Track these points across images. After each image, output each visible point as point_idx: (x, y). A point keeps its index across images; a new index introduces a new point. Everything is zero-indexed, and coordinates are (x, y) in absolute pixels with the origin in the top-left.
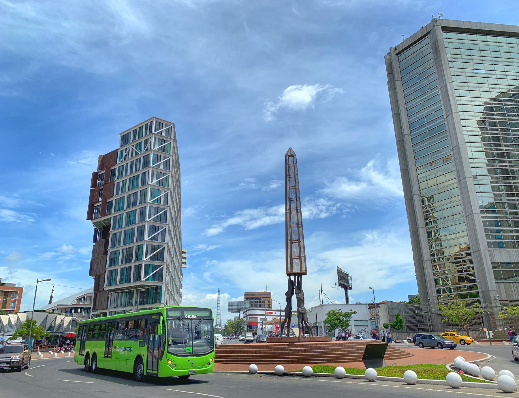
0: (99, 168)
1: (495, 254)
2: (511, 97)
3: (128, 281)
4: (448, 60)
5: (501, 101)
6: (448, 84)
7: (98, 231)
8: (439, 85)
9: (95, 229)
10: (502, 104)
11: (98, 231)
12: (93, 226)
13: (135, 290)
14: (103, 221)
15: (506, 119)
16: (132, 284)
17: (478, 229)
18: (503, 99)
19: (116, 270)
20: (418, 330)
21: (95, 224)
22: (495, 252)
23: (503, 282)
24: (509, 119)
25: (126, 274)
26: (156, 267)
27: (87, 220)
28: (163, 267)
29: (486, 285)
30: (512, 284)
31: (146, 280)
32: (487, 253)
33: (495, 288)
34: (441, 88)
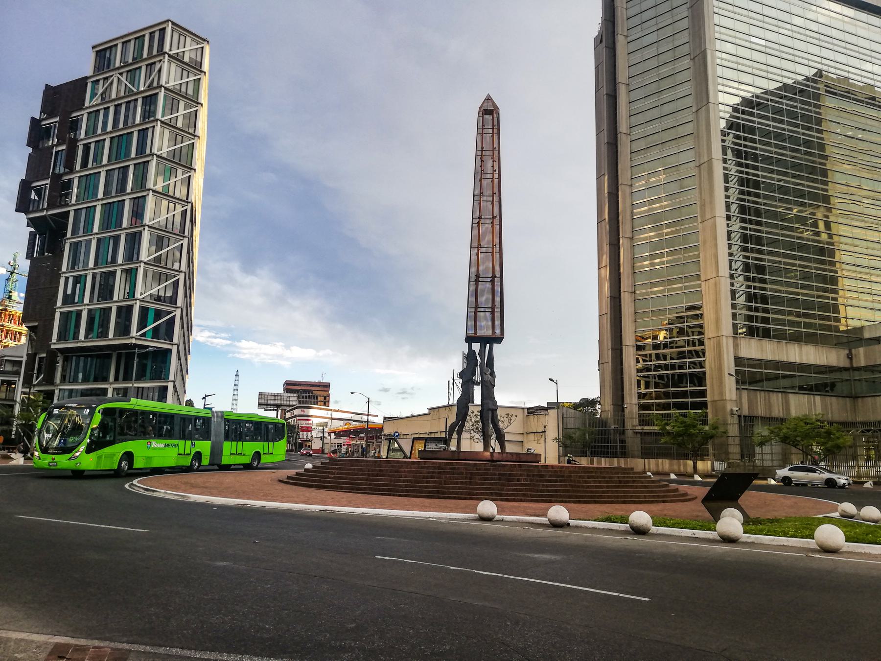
0: (43, 111)
1: (742, 343)
2: (795, 94)
3: (104, 334)
4: (714, 11)
5: (781, 98)
6: (709, 52)
7: (38, 236)
8: (692, 53)
10: (782, 103)
11: (38, 236)
12: (28, 225)
13: (114, 353)
14: (49, 217)
15: (784, 129)
16: (112, 338)
17: (723, 301)
18: (785, 96)
19: (79, 314)
21: (32, 222)
23: (746, 389)
24: (789, 131)
25: (98, 322)
26: (158, 314)
27: (17, 211)
28: (175, 315)
29: (722, 393)
30: (758, 392)
31: (140, 335)
32: (731, 341)
33: (734, 397)
34: (694, 58)
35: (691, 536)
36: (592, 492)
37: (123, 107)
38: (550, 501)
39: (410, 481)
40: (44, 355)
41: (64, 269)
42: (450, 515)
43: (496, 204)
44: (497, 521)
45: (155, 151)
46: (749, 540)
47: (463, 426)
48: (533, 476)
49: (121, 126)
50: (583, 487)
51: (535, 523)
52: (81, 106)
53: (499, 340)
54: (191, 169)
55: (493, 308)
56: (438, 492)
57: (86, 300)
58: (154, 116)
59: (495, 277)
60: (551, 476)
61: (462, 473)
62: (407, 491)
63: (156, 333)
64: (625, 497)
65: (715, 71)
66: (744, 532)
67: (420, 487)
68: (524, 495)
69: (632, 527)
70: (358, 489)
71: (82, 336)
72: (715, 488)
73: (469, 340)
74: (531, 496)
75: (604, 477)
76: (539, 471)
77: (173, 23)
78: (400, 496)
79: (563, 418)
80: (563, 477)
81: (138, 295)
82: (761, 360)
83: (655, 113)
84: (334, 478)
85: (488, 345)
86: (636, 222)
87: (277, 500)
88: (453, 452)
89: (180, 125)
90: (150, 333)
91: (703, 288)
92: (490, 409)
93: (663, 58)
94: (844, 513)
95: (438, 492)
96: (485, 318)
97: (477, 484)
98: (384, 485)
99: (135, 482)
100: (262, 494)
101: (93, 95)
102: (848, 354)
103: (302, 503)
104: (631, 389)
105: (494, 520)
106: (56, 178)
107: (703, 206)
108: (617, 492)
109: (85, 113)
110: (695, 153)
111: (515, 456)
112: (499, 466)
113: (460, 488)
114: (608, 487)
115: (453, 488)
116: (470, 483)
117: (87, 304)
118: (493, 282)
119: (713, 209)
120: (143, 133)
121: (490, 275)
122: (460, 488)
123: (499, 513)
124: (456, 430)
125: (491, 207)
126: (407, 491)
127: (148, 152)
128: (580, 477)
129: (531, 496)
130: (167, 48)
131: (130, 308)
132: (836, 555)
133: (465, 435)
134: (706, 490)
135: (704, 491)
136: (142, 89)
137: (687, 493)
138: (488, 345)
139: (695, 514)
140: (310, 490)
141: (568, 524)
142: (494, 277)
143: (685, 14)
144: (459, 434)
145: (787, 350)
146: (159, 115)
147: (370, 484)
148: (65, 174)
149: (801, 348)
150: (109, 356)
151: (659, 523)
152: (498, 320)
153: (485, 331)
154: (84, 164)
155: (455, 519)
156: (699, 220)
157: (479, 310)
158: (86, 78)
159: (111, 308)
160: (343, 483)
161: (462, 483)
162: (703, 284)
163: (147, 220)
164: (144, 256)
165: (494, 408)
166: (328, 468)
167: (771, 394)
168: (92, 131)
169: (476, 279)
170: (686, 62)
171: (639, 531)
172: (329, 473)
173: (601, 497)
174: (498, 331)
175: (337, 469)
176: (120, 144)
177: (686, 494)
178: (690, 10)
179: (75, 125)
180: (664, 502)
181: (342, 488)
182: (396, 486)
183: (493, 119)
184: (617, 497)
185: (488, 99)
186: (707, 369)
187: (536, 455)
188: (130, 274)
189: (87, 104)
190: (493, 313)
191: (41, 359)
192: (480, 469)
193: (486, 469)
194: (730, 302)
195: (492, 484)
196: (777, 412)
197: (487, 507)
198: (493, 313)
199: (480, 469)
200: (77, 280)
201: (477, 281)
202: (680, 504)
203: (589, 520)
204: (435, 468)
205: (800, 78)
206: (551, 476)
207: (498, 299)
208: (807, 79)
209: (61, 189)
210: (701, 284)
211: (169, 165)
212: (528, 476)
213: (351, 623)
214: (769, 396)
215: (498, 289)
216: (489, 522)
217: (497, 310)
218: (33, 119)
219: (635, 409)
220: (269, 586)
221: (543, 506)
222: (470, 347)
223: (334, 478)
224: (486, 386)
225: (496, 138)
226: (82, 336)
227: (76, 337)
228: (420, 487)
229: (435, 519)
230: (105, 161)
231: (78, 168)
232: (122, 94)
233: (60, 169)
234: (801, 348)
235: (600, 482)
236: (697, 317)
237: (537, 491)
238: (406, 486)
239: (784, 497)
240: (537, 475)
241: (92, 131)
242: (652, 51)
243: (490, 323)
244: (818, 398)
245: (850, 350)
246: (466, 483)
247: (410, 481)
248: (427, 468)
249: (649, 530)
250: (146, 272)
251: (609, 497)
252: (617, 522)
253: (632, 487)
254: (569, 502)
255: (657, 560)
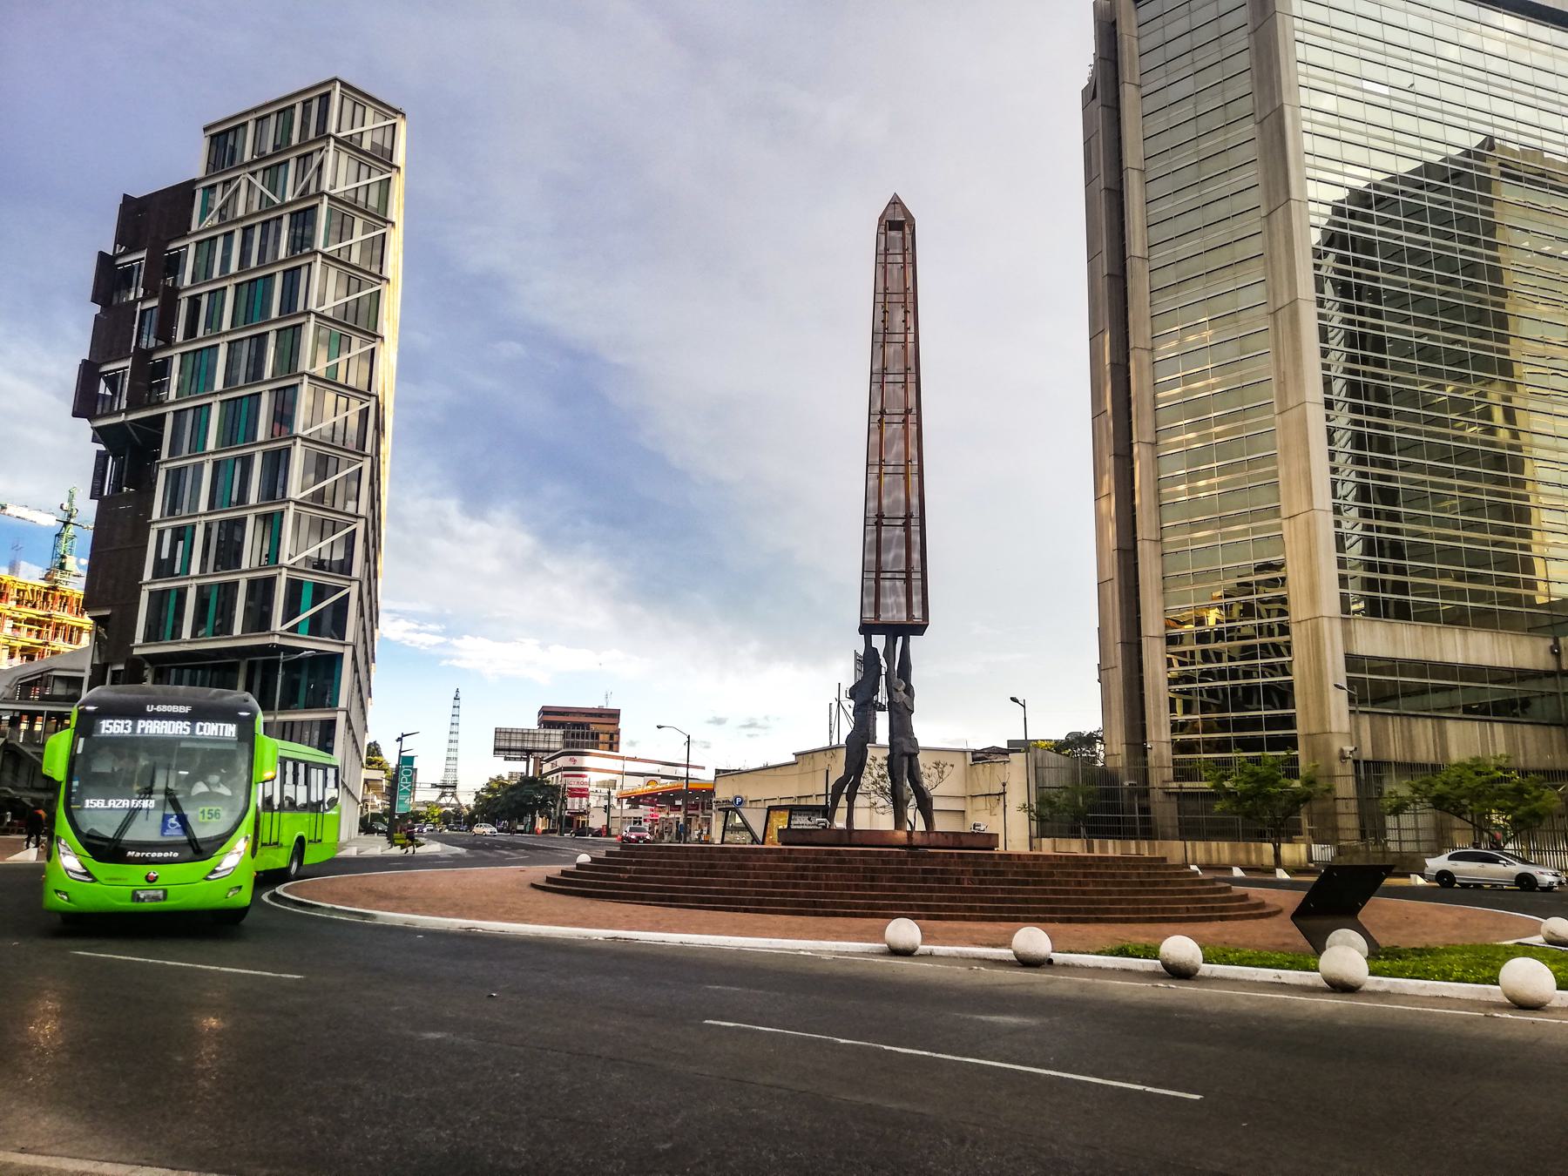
0: (119, 240)
1: (1357, 627)
2: (1446, 181)
3: (225, 628)
5: (1421, 188)
6: (1288, 110)
9: (99, 453)
10: (1421, 197)
12: (94, 440)
15: (1427, 244)
16: (239, 637)
18: (1428, 185)
19: (181, 593)
20: (1120, 833)
21: (100, 435)
22: (1357, 624)
24: (1436, 246)
25: (214, 608)
26: (320, 592)
27: (75, 415)
28: (348, 594)
29: (1323, 719)
30: (1390, 718)
31: (288, 630)
32: (1337, 625)
34: (1261, 121)
35: (1274, 980)
36: (1092, 902)
37: (258, 231)
38: (1016, 920)
39: (764, 885)
40: (121, 667)
41: (156, 515)
42: (837, 946)
43: (912, 387)
44: (920, 955)
45: (313, 306)
46: (1380, 988)
47: (857, 784)
48: (986, 873)
49: (253, 263)
50: (1075, 892)
51: (991, 960)
52: (183, 231)
53: (920, 629)
54: (375, 336)
55: (908, 572)
56: (815, 904)
57: (195, 569)
58: (311, 246)
59: (911, 516)
60: (1016, 873)
61: (857, 870)
62: (760, 903)
63: (315, 626)
64: (1151, 911)
65: (1299, 143)
66: (1372, 973)
67: (782, 894)
68: (971, 909)
69: (1165, 965)
70: (671, 899)
71: (186, 633)
72: (1315, 892)
73: (867, 630)
74: (982, 909)
75: (1113, 875)
76: (996, 864)
77: (343, 84)
78: (746, 911)
79: (1037, 771)
80: (1039, 874)
81: (284, 559)
82: (1394, 660)
83: (1194, 220)
84: (629, 879)
85: (900, 639)
86: (1161, 414)
87: (530, 920)
88: (840, 831)
89: (355, 260)
90: (305, 628)
91: (1285, 532)
92: (904, 754)
93: (1205, 124)
94: (1554, 938)
95: (815, 904)
96: (894, 590)
97: (883, 888)
98: (717, 892)
99: (279, 890)
100: (501, 910)
101: (206, 211)
102: (1552, 648)
103: (574, 924)
104: (1158, 715)
105: (917, 953)
106: (142, 356)
107: (1282, 384)
108: (1135, 901)
109: (191, 243)
110: (1268, 291)
111: (951, 836)
112: (924, 855)
113: (853, 897)
114: (1120, 893)
115: (841, 896)
116: (872, 888)
117: (196, 576)
118: (907, 526)
119: (1300, 387)
120: (292, 276)
121: (902, 514)
122: (853, 897)
123: (925, 940)
124: (845, 791)
125: (902, 393)
126: (760, 903)
127: (300, 308)
128: (1069, 875)
129: (982, 909)
130: (332, 128)
131: (270, 583)
132: (1539, 1013)
133: (860, 801)
134: (1298, 896)
135: (1293, 899)
136: (289, 198)
137: (1264, 903)
138: (900, 639)
139: (1279, 940)
140: (587, 901)
141: (1050, 961)
142: (908, 517)
143: (1244, 44)
144: (851, 798)
145: (1440, 642)
146: (319, 244)
147: (693, 891)
148: (158, 349)
149: (1465, 639)
150: (234, 668)
151: (1215, 958)
152: (917, 594)
153: (894, 612)
154: (191, 332)
155: (846, 953)
156: (1276, 411)
157: (882, 575)
158: (194, 182)
159: (236, 583)
160: (645, 889)
161: (857, 887)
162: (1285, 523)
163: (299, 429)
164: (295, 490)
165: (912, 751)
166: (619, 862)
167: (1413, 720)
168: (203, 273)
169: (877, 521)
170: (1248, 128)
171: (1179, 972)
172: (620, 871)
173: (1108, 911)
174: (917, 614)
175: (630, 863)
176: (253, 297)
177: (1261, 905)
178: (1252, 36)
179: (174, 264)
180: (1222, 919)
181: (643, 898)
182: (739, 893)
183: (904, 238)
184: (1138, 911)
185: (895, 202)
186: (1296, 677)
187: (990, 835)
188: (271, 523)
189: (194, 228)
190: (908, 581)
191: (114, 672)
192: (888, 863)
193: (900, 862)
194: (1334, 555)
195: (910, 889)
196: (1424, 748)
197: (904, 931)
198: (908, 581)
199: (888, 863)
200: (179, 534)
201: (879, 525)
202: (1251, 924)
203: (1088, 953)
204: (807, 860)
205: (1454, 152)
206: (1016, 873)
207: (916, 556)
208: (1468, 153)
209: (150, 376)
210: (1281, 524)
211: (338, 330)
212: (976, 873)
213: (665, 1142)
214: (1409, 724)
215: (916, 538)
216: (908, 958)
217: (916, 576)
218: (102, 255)
219: (1167, 751)
220: (517, 1075)
221: (1001, 928)
222: (868, 642)
223: (629, 879)
224: (898, 713)
225: (910, 270)
226: (186, 633)
227: (176, 634)
228: (782, 894)
229: (809, 954)
230: (226, 326)
231: (179, 338)
232: (255, 208)
233: (149, 342)
234: (1465, 639)
235: (1106, 884)
236: (1274, 583)
237: (993, 900)
238: (757, 893)
239: (1439, 909)
240: (992, 873)
241: (203, 273)
242: (1186, 111)
243: (903, 600)
244: (1499, 728)
245: (1556, 641)
246: (864, 888)
247: (764, 885)
248: (796, 860)
249: (1197, 970)
250: (297, 518)
251: (1122, 911)
252: (1139, 957)
253: (1163, 892)
254: (1051, 920)
255: (1212, 1026)
